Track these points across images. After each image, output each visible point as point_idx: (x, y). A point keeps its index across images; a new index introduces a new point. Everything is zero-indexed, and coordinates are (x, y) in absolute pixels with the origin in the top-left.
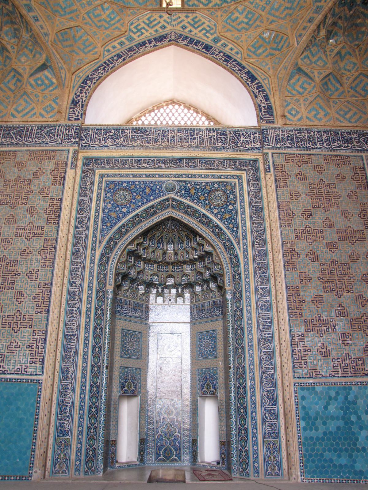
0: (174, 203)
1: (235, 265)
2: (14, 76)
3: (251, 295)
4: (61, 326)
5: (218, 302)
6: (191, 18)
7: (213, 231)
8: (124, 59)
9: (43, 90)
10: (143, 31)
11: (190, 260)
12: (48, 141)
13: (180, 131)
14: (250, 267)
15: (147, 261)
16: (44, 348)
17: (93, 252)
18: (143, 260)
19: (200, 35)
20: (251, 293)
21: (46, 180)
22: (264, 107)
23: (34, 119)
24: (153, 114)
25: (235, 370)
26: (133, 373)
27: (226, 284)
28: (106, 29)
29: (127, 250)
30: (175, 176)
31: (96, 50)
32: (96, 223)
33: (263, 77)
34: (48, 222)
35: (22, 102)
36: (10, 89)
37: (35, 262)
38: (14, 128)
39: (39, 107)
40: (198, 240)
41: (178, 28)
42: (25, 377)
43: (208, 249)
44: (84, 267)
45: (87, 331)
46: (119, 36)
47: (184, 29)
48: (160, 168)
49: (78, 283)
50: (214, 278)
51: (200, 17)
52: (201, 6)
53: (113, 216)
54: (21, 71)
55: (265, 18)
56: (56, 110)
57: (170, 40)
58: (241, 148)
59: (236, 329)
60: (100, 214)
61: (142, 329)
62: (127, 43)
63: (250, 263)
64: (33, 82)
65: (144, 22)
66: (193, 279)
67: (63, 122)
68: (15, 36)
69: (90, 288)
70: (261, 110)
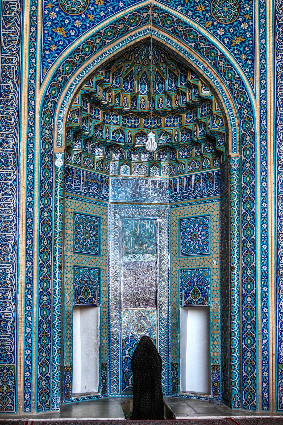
0: (156, 15)
1: (246, 119)
3: (269, 166)
5: (214, 174)
7: (215, 65)
11: (173, 110)
14: (269, 124)
15: (109, 110)
17: (32, 92)
18: (101, 109)
20: (269, 162)
25: (241, 272)
26: (91, 274)
27: (230, 149)
29: (81, 92)
32: (33, 45)
40: (189, 78)
43: (205, 93)
44: (19, 116)
49: (11, 142)
50: (210, 139)
53: (59, 33)
59: (244, 215)
60: (39, 28)
61: (101, 212)
63: (269, 118)
66: (175, 140)
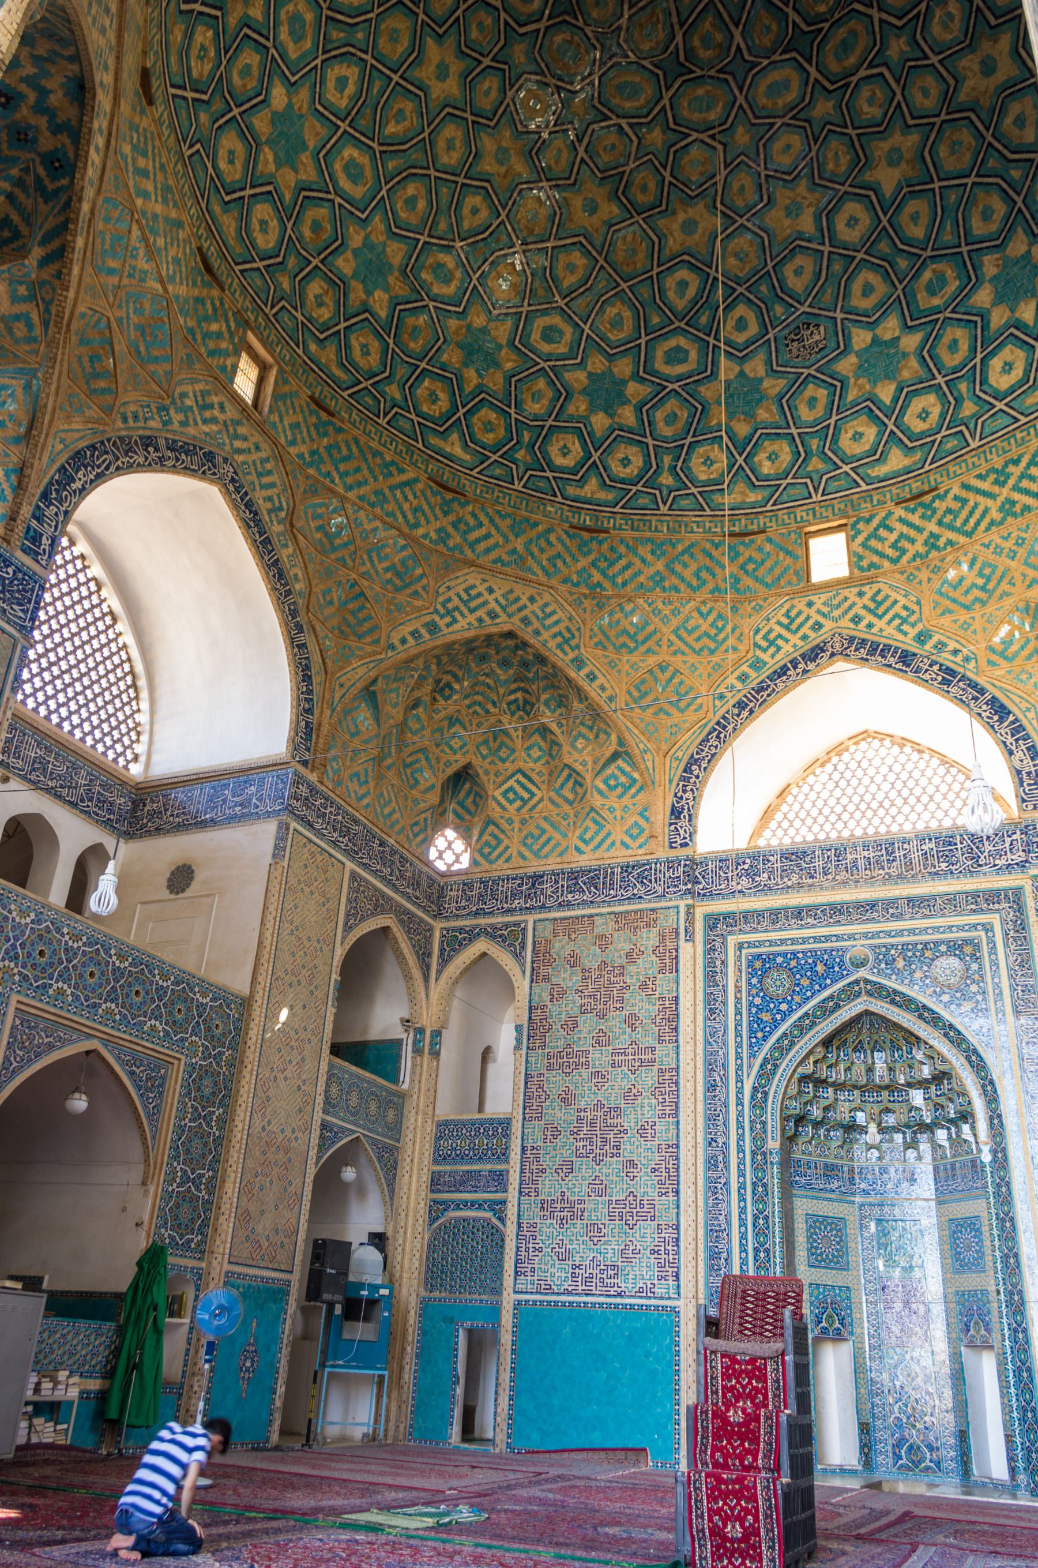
2: (569, 776)
4: (701, 1215)
6: (869, 595)
8: (751, 712)
9: (621, 796)
10: (780, 642)
12: (641, 893)
13: (866, 848)
15: (839, 1086)
16: (677, 1253)
19: (890, 630)
21: (647, 964)
22: (1029, 773)
23: (613, 853)
24: (829, 768)
28: (712, 652)
30: (865, 936)
31: (699, 701)
33: (1024, 705)
34: (660, 1041)
35: (589, 823)
36: (566, 800)
37: (648, 1109)
38: (584, 872)
39: (618, 828)
41: (845, 622)
42: (653, 1302)
44: (727, 1112)
45: (742, 1223)
46: (737, 664)
47: (856, 623)
48: (838, 923)
49: (720, 1141)
51: (886, 590)
52: (886, 564)
54: (579, 768)
55: (1018, 576)
56: (647, 833)
57: (833, 655)
58: (985, 869)
59: (1003, 1220)
62: (753, 674)
64: (602, 786)
65: (779, 623)
67: (663, 853)
68: (560, 704)
69: (741, 1149)
70: (1021, 782)
